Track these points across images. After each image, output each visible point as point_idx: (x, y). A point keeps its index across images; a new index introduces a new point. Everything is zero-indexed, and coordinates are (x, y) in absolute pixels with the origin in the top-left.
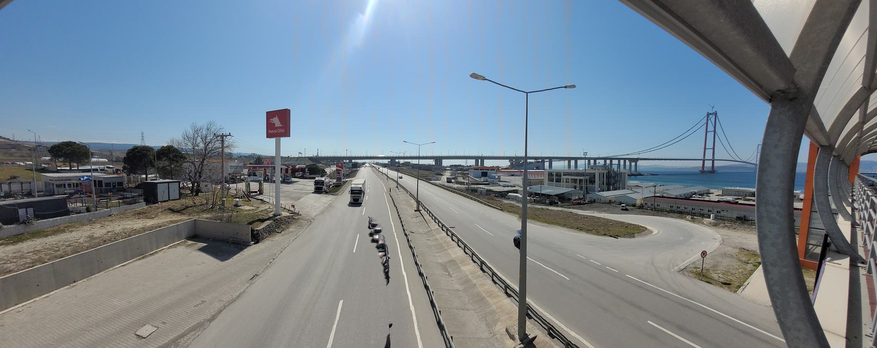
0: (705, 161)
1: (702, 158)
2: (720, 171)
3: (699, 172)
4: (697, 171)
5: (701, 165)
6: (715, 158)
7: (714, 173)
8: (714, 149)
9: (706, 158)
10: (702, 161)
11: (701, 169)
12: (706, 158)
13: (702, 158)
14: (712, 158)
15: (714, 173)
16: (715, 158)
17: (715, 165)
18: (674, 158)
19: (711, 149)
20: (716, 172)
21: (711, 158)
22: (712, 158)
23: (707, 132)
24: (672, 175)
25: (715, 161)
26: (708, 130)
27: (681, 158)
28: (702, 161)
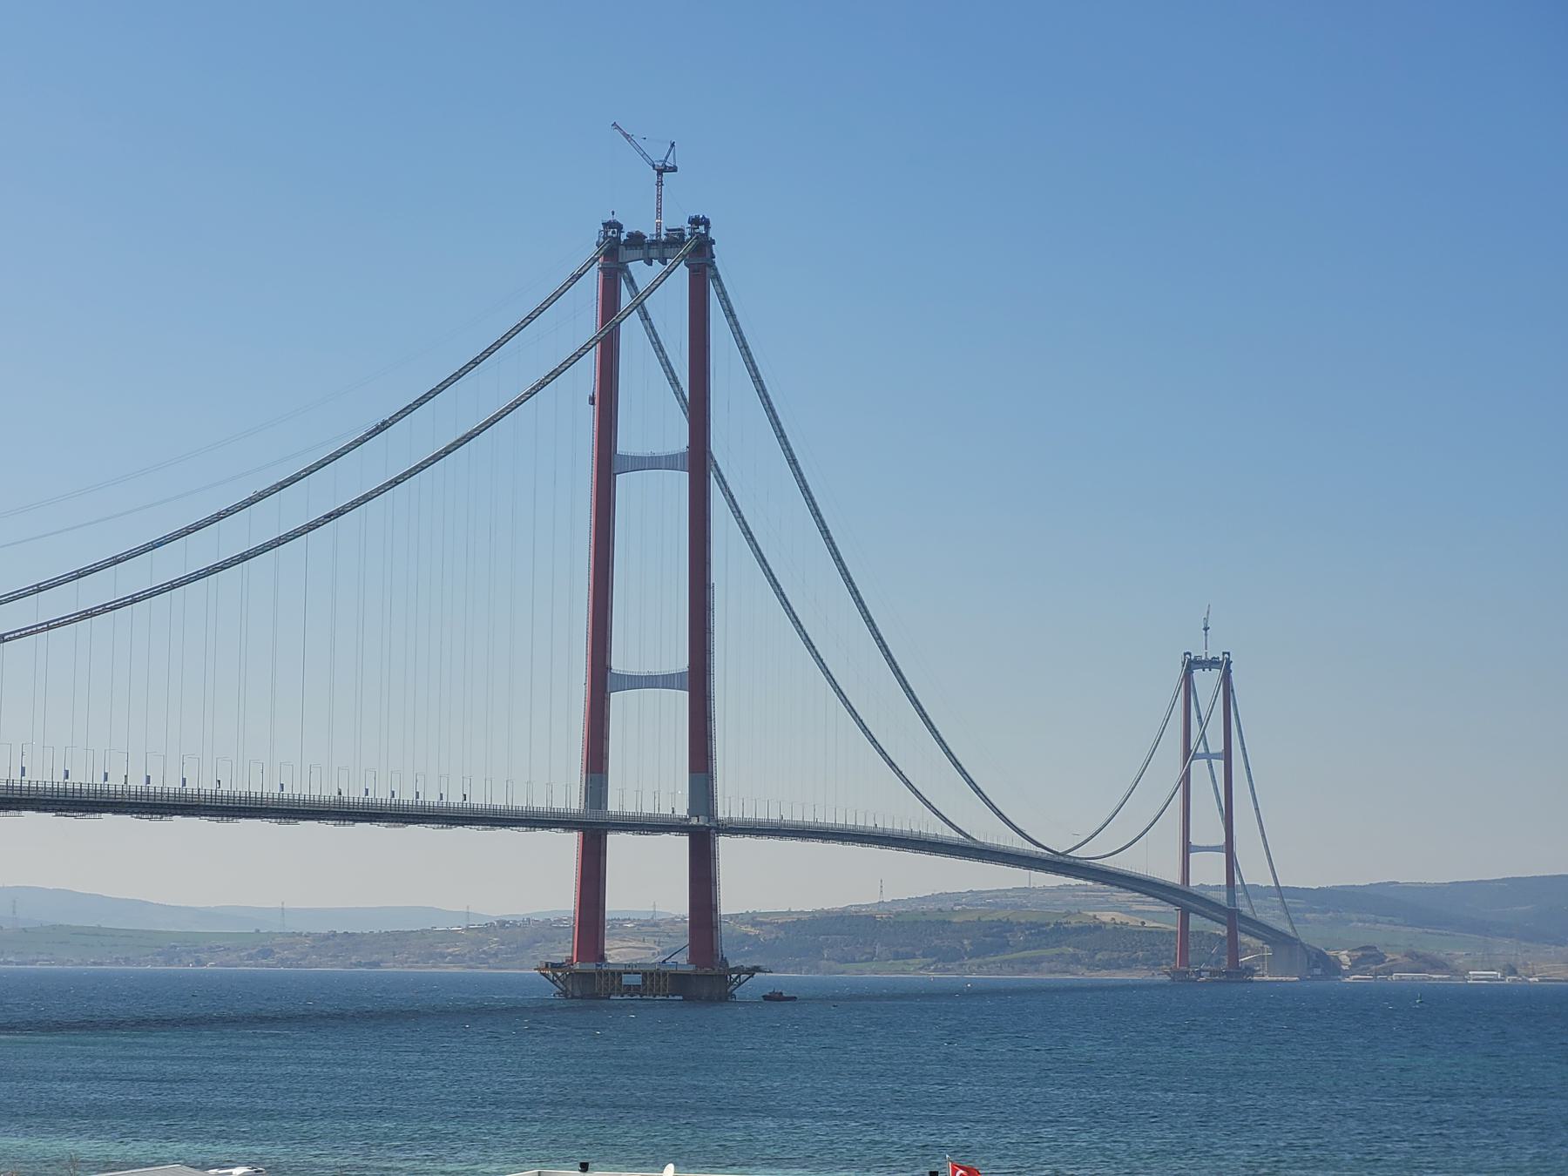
0: (617, 844)
1: (570, 798)
2: (782, 977)
3: (551, 991)
4: (526, 969)
5: (564, 901)
6: (726, 808)
7: (725, 997)
8: (698, 681)
9: (614, 806)
10: (573, 839)
11: (564, 951)
12: (614, 806)
13: (570, 798)
14: (682, 810)
15: (725, 997)
16: (726, 808)
17: (732, 900)
18: (202, 783)
19: (665, 681)
20: (751, 988)
21: (676, 801)
22: (682, 810)
23: (607, 465)
24: (141, 1024)
25: (726, 846)
26: (627, 443)
27: (301, 788)
28: (573, 839)
